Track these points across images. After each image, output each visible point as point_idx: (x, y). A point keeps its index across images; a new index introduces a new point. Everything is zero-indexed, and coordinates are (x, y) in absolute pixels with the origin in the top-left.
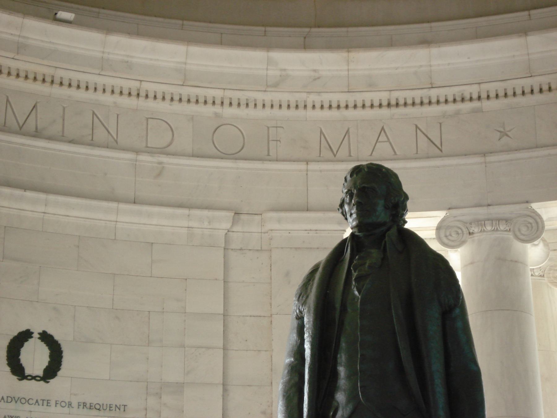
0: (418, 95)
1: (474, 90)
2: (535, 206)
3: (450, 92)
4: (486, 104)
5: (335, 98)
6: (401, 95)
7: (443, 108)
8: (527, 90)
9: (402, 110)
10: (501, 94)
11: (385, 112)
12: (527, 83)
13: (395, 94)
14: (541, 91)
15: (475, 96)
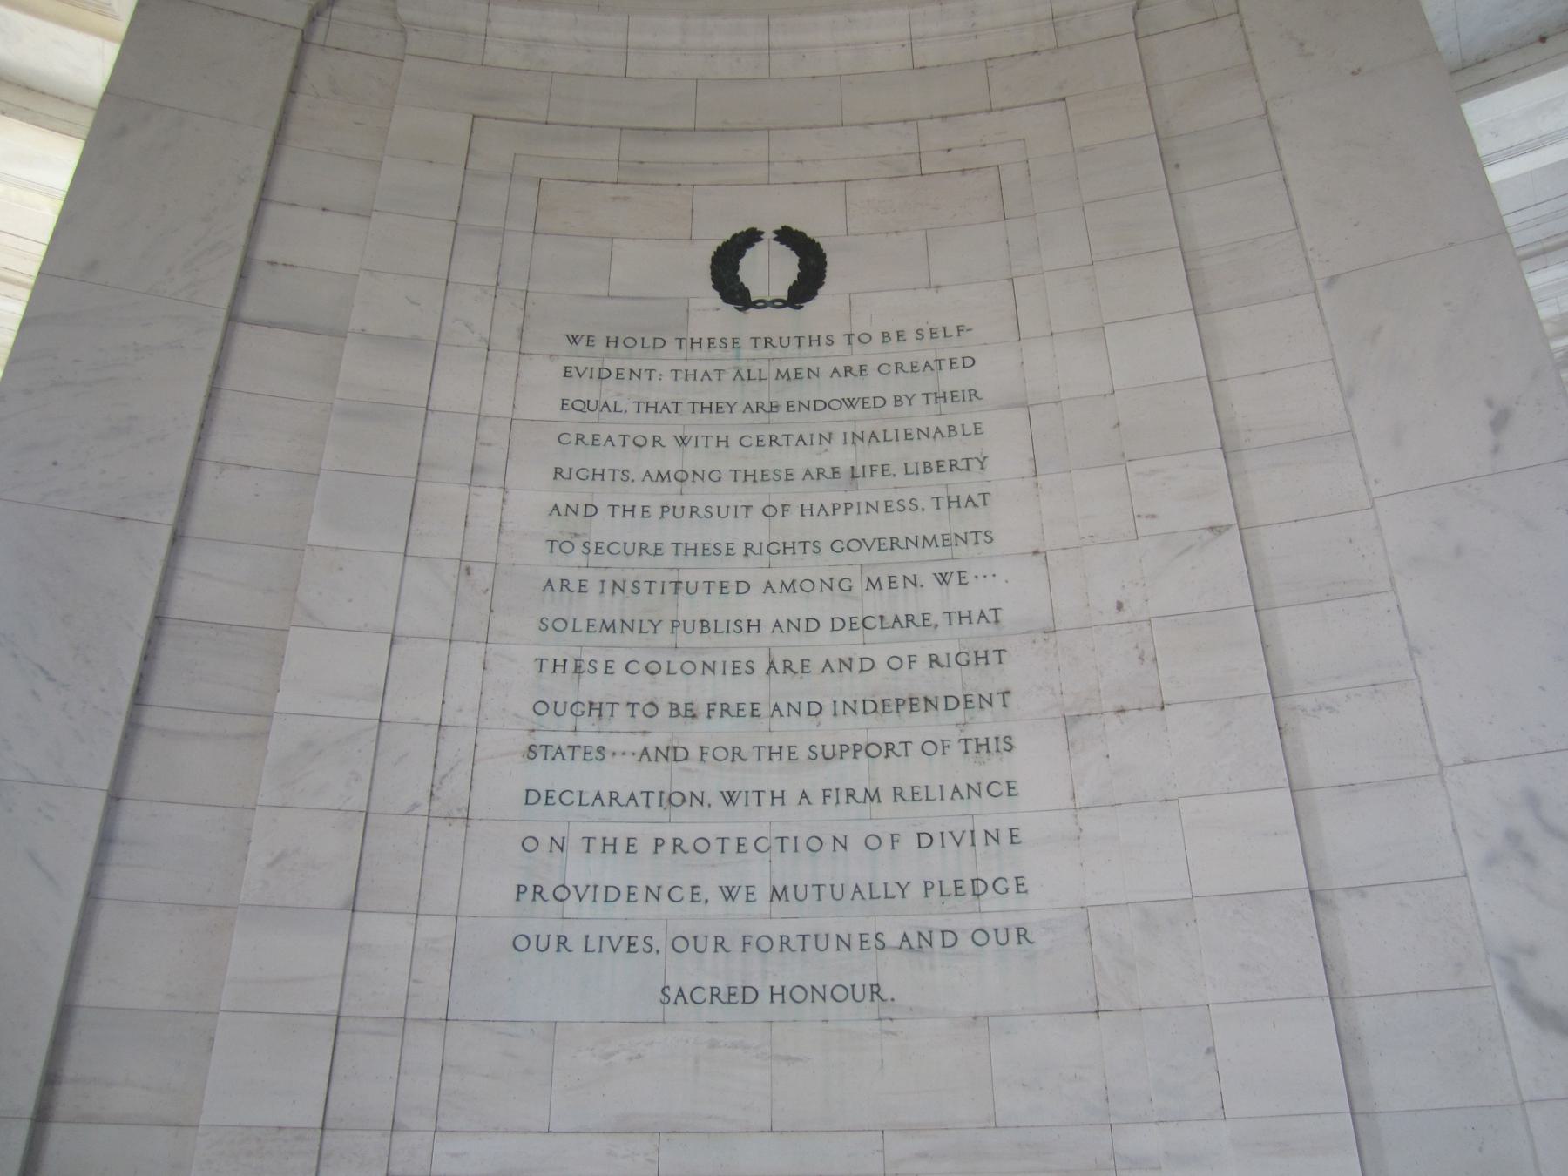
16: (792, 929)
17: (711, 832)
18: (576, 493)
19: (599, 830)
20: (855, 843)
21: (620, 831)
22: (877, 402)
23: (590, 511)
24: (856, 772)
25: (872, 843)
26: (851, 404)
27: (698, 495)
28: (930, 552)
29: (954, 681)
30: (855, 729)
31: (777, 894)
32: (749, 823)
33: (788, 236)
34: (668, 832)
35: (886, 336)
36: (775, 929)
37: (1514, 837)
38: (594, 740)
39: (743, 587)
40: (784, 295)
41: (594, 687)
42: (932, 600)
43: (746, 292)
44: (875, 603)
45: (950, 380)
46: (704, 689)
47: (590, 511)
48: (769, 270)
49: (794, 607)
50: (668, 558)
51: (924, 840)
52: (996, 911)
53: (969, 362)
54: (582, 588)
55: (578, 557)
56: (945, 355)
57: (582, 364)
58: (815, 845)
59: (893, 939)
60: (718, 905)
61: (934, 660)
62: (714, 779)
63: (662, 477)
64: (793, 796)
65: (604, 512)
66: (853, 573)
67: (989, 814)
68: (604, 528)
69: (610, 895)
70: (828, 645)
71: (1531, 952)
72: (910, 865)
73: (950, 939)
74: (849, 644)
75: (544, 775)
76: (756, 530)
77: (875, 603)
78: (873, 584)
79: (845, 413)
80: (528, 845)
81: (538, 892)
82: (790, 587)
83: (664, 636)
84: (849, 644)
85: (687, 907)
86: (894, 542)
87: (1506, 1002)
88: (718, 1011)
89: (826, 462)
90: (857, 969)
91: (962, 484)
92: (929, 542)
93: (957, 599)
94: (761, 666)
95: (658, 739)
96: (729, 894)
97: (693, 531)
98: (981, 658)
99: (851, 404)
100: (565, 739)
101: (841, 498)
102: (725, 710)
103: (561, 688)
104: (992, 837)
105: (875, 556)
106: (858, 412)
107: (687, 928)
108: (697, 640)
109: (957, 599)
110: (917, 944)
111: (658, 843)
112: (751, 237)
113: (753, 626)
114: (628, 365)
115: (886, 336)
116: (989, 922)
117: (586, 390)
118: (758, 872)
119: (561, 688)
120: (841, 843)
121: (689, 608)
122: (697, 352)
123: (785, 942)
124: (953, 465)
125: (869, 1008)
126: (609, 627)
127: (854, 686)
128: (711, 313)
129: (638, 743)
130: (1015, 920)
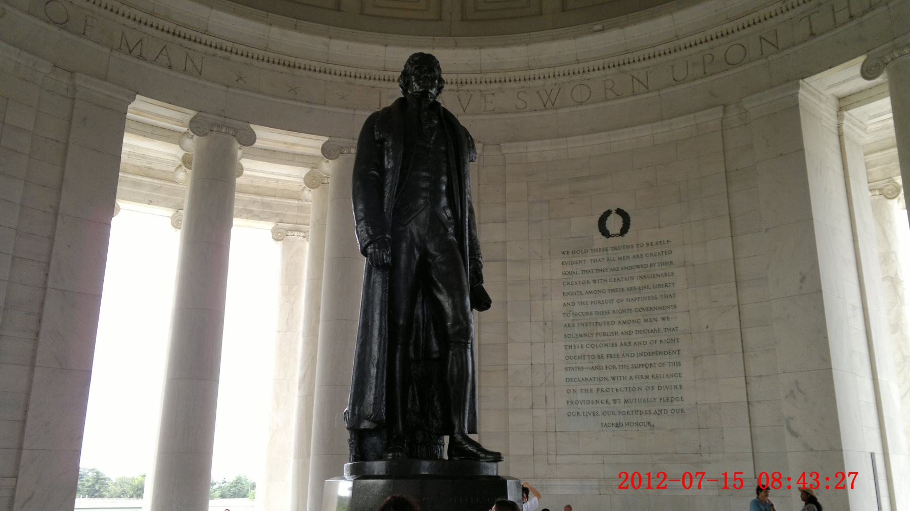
0: (194, 34)
1: (229, 45)
2: (252, 126)
3: (215, 41)
4: (233, 57)
5: (140, 15)
6: (183, 31)
7: (207, 48)
8: (261, 58)
9: (181, 40)
10: (245, 54)
11: (170, 36)
12: (262, 53)
13: (180, 28)
14: (268, 61)
15: (229, 49)
16: (629, 409)
17: (609, 386)
18: (569, 299)
19: (583, 387)
20: (643, 389)
21: (589, 387)
22: (645, 266)
23: (573, 304)
24: (643, 371)
25: (647, 389)
26: (638, 267)
27: (601, 297)
28: (661, 311)
29: (666, 347)
30: (642, 360)
31: (626, 401)
32: (619, 384)
33: (620, 212)
34: (600, 387)
35: (647, 244)
36: (626, 410)
37: (792, 392)
38: (581, 365)
39: (613, 323)
40: (619, 232)
41: (579, 352)
42: (661, 325)
43: (608, 232)
44: (647, 326)
45: (666, 258)
46: (605, 351)
47: (573, 304)
48: (614, 224)
49: (626, 328)
50: (594, 316)
51: (660, 388)
52: (676, 405)
53: (670, 252)
54: (574, 325)
55: (572, 318)
56: (664, 250)
57: (566, 260)
58: (634, 389)
59: (653, 412)
60: (612, 404)
61: (661, 341)
62: (609, 374)
63: (591, 292)
64: (628, 377)
65: (577, 304)
66: (640, 317)
67: (675, 381)
68: (577, 309)
69: (588, 402)
70: (635, 338)
71: (792, 419)
72: (657, 394)
73: (666, 411)
74: (640, 338)
75: (571, 374)
76: (616, 306)
77: (647, 326)
78: (646, 321)
79: (637, 270)
80: (568, 391)
81: (572, 402)
82: (624, 322)
83: (595, 338)
84: (640, 338)
85: (606, 405)
86: (651, 308)
87: (786, 431)
88: (614, 428)
89: (632, 285)
90: (645, 418)
91: (668, 291)
92: (660, 308)
93: (667, 324)
94: (619, 344)
95: (595, 364)
96: (615, 402)
97: (600, 308)
98: (673, 341)
99: (638, 267)
100: (574, 365)
101: (637, 296)
102: (611, 356)
103: (571, 352)
104: (676, 387)
105: (646, 313)
106: (641, 269)
107: (606, 410)
108: (603, 338)
109: (667, 324)
110: (659, 412)
111: (598, 390)
112: (608, 213)
113: (616, 333)
114: (579, 259)
115: (647, 244)
116: (675, 408)
117: (569, 268)
118: (621, 396)
119: (571, 352)
120: (640, 389)
121: (600, 329)
122: (596, 253)
123: (628, 412)
124: (666, 285)
125: (648, 427)
126: (581, 336)
127: (642, 349)
128: (599, 240)
129: (591, 365)
130: (680, 407)
